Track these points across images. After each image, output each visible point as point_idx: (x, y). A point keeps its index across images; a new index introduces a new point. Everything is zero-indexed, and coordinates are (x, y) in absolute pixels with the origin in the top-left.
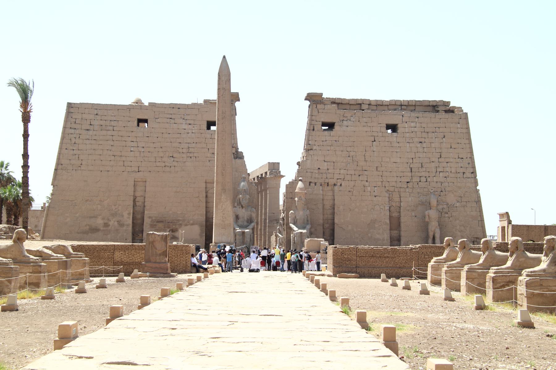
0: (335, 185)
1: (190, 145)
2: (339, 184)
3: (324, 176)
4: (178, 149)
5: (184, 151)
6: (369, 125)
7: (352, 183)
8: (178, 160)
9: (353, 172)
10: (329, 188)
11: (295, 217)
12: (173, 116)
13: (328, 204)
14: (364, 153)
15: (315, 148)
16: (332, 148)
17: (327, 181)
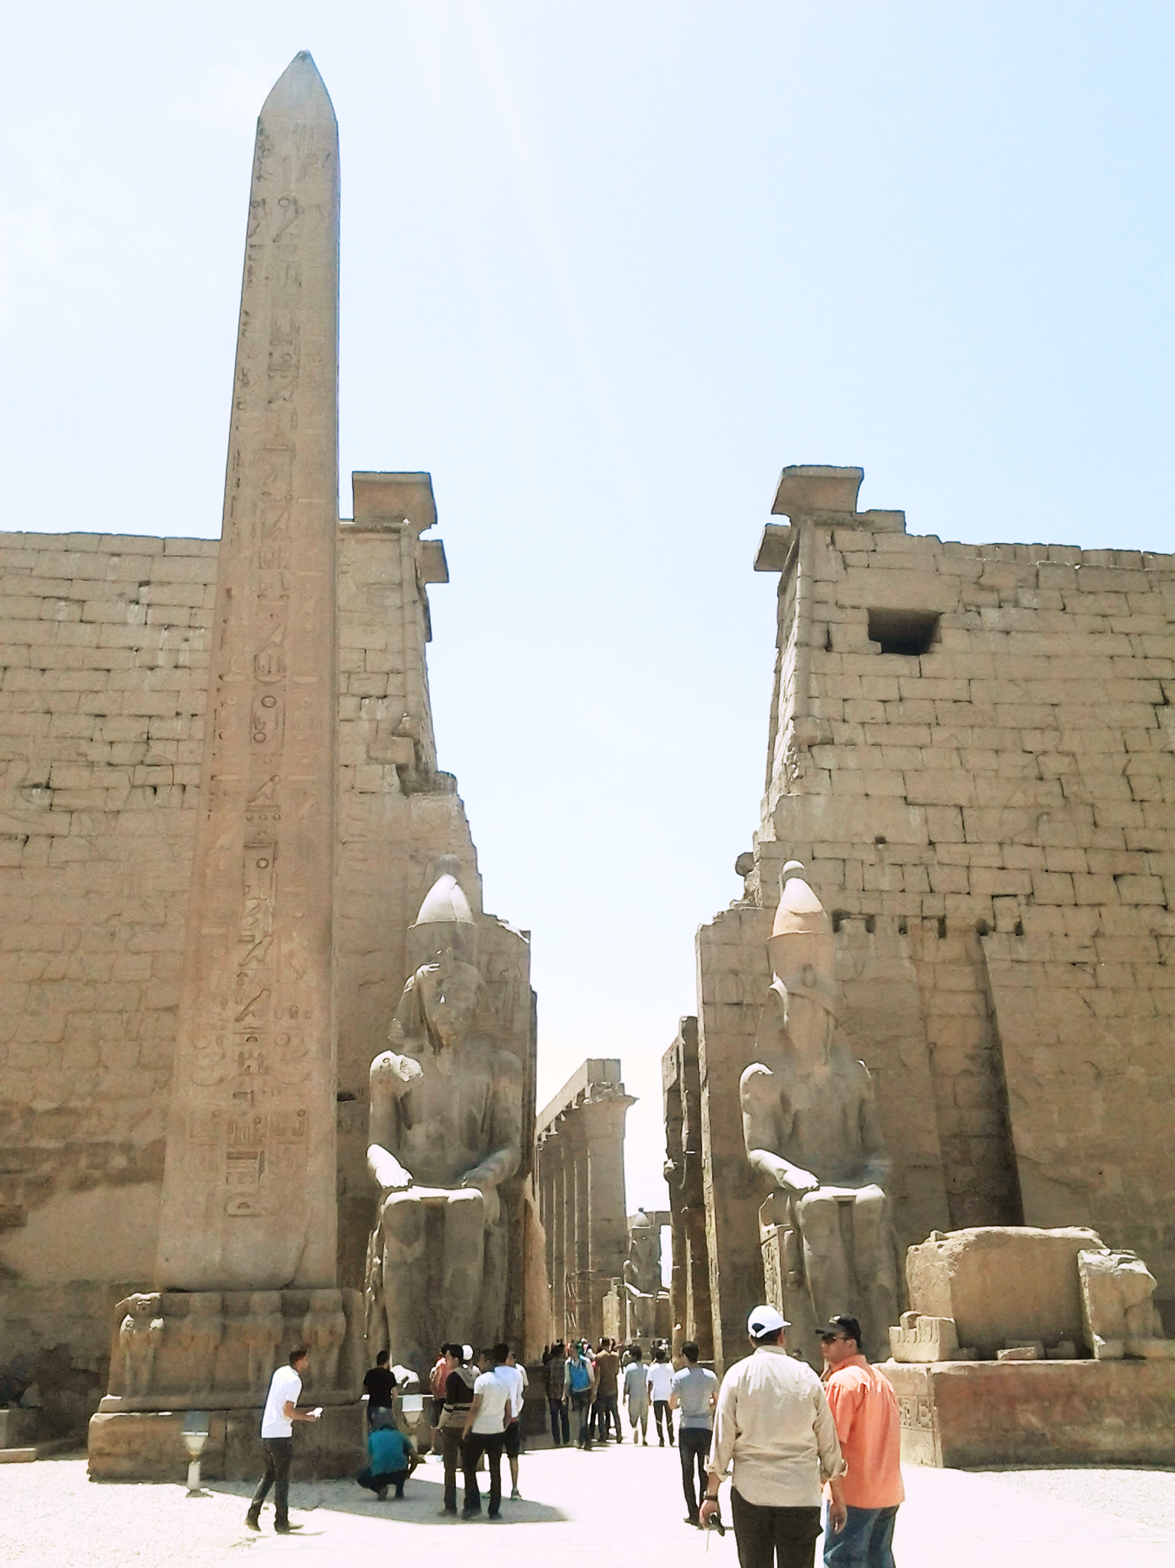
0: (983, 931)
1: (156, 723)
2: (1006, 924)
3: (915, 879)
4: (84, 746)
5: (121, 754)
6: (1119, 625)
7: (1082, 921)
8: (77, 803)
9: (1075, 860)
10: (952, 947)
11: (784, 1101)
12: (77, 591)
13: (958, 1042)
14: (1120, 761)
15: (843, 733)
16: (940, 734)
17: (934, 906)
